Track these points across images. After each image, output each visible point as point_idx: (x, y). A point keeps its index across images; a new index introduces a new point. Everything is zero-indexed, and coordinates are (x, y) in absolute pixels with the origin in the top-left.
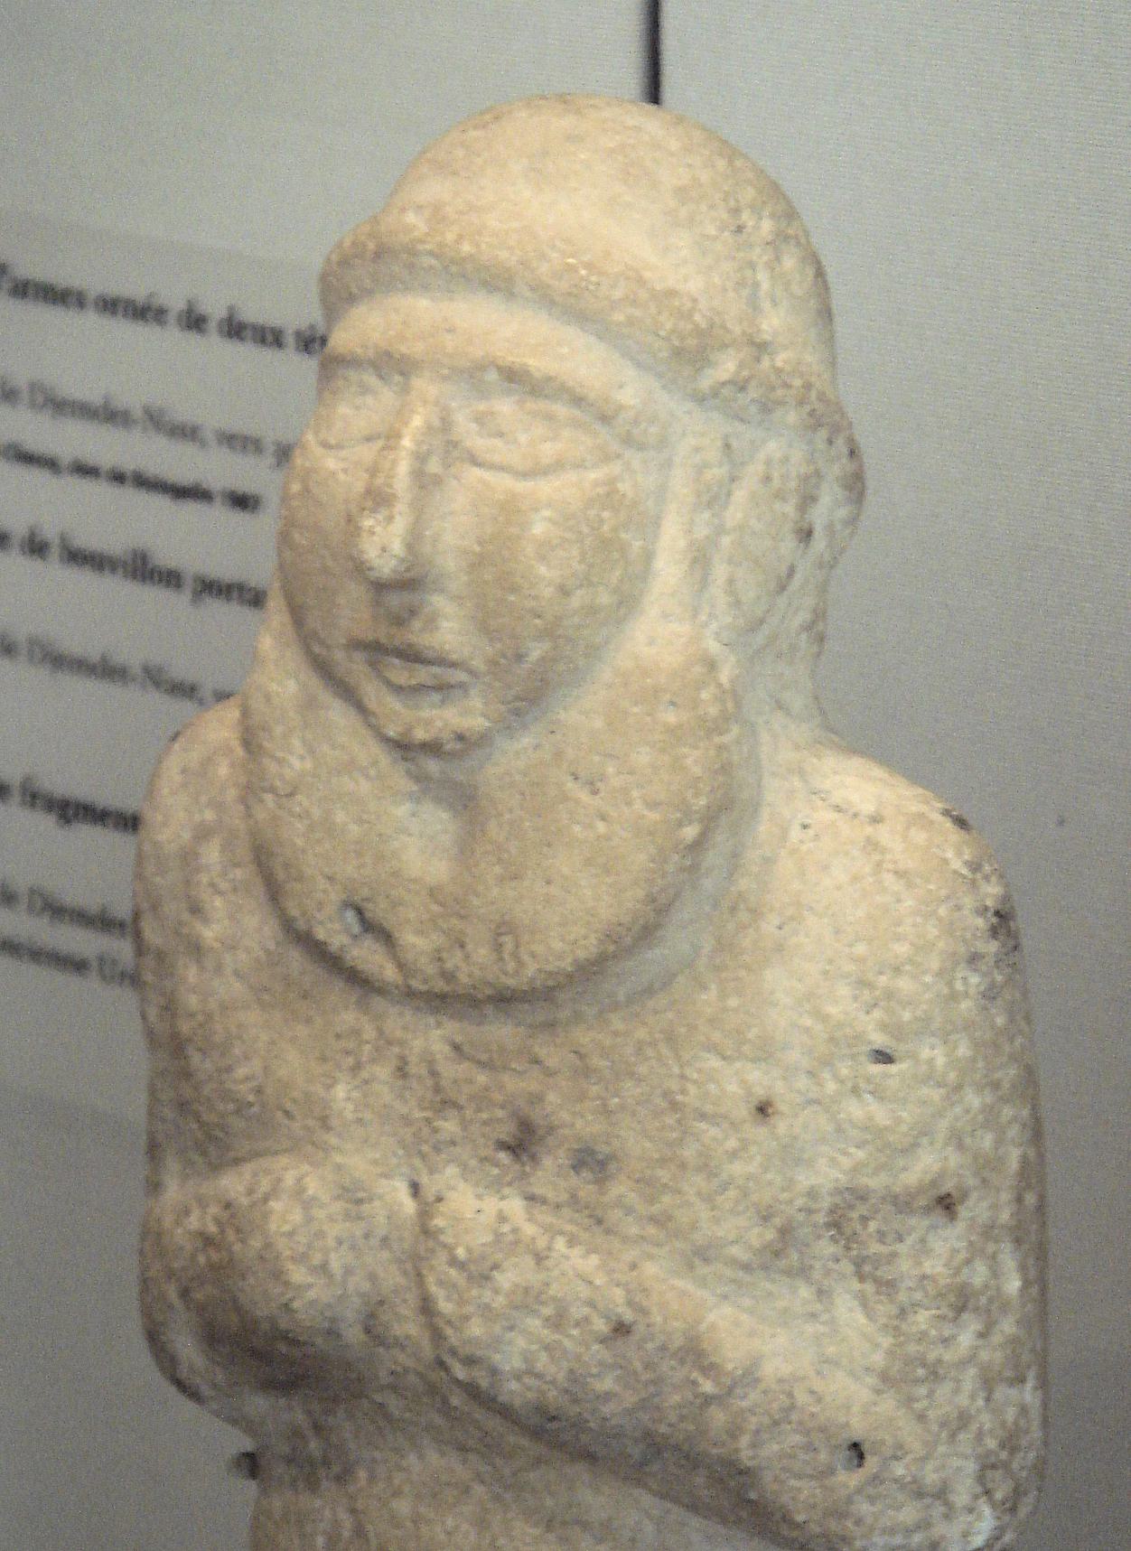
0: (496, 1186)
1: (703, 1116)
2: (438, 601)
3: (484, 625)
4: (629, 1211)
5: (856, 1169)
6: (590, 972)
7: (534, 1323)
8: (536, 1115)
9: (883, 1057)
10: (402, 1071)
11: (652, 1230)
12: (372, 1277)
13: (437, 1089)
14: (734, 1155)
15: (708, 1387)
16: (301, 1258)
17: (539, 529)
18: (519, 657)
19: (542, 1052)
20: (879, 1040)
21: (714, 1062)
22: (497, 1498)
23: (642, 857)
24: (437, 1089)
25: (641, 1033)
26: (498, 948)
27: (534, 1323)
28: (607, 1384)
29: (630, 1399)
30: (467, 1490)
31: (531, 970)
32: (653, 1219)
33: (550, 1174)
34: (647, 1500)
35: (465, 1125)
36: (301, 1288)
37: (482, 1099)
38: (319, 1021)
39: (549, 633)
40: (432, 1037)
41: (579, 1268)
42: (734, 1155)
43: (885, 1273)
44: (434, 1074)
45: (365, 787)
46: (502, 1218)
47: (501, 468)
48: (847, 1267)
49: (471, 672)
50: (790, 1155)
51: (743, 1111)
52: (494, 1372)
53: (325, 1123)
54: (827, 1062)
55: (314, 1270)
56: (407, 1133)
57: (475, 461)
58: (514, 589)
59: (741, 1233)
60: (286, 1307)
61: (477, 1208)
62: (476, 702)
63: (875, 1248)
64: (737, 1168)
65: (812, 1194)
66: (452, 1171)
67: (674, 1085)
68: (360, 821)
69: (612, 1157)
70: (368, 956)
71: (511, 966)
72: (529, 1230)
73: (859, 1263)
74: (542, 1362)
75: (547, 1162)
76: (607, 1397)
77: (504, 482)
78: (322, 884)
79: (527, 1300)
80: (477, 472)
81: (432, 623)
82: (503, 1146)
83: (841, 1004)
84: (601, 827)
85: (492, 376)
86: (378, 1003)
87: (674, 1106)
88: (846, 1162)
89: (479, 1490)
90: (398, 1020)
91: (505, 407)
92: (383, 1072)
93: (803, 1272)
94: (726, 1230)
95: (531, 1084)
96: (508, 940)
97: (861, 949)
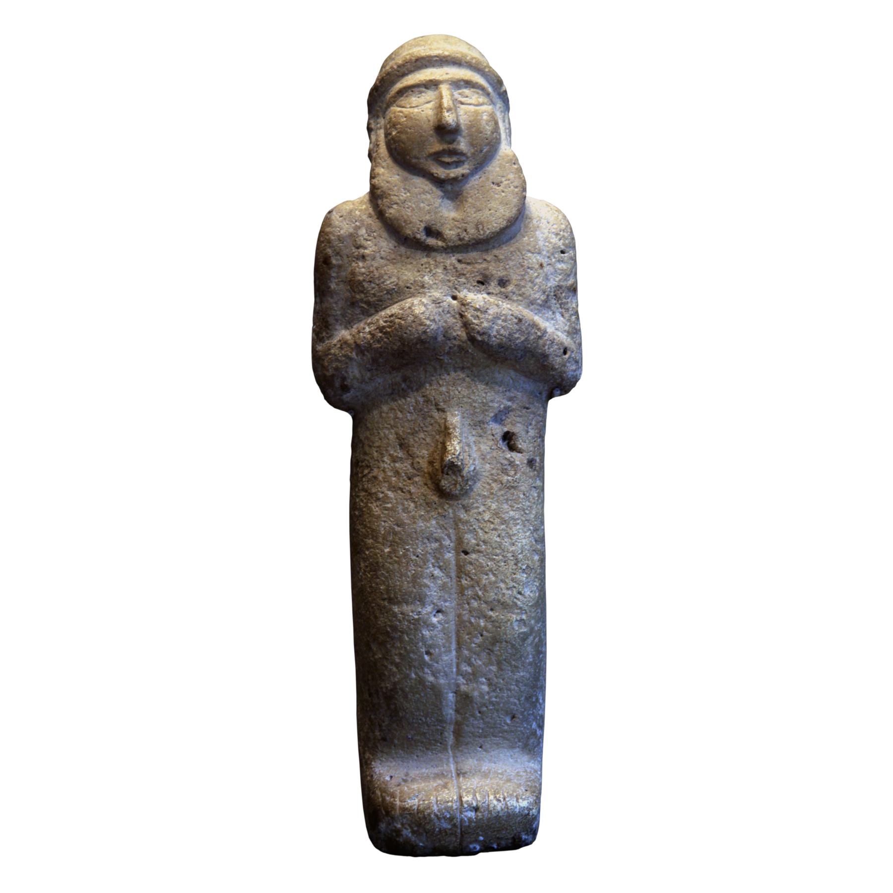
0: (480, 292)
1: (529, 268)
2: (460, 138)
3: (472, 144)
4: (514, 293)
5: (560, 281)
6: (503, 231)
7: (500, 322)
8: (487, 273)
9: (563, 252)
10: (445, 268)
11: (520, 298)
12: (446, 322)
13: (457, 271)
14: (537, 277)
15: (539, 334)
16: (428, 319)
17: (485, 117)
18: (481, 151)
19: (485, 257)
20: (563, 247)
21: (529, 254)
22: (473, 380)
23: (515, 200)
24: (457, 271)
25: (511, 249)
26: (477, 229)
27: (500, 322)
28: (517, 335)
29: (523, 338)
30: (464, 380)
31: (488, 232)
32: (520, 295)
33: (493, 287)
34: (512, 373)
35: (466, 278)
36: (429, 326)
37: (472, 272)
38: (414, 263)
39: (488, 144)
40: (452, 260)
41: (506, 307)
42: (537, 277)
43: (566, 307)
44: (455, 268)
45: (429, 196)
46: (484, 298)
47: (470, 104)
48: (558, 306)
49: (467, 158)
50: (547, 278)
51: (537, 266)
52: (489, 335)
53: (423, 287)
54: (553, 254)
55: (431, 321)
56: (450, 284)
57: (462, 103)
58: (481, 133)
59: (540, 297)
60: (425, 332)
61: (476, 298)
62: (466, 166)
63: (564, 300)
64: (538, 280)
65: (550, 287)
66: (465, 291)
67: (521, 261)
68: (429, 205)
69: (509, 281)
70: (431, 241)
71: (482, 232)
72: (492, 300)
73: (561, 304)
74: (502, 332)
75: (492, 284)
76: (518, 338)
77: (472, 108)
78: (418, 223)
79: (497, 317)
80: (462, 106)
81: (459, 143)
82: (479, 282)
83: (555, 240)
84: (503, 194)
85: (462, 83)
86: (433, 254)
87: (522, 266)
88: (557, 279)
89: (467, 379)
90: (440, 258)
91: (467, 91)
92: (439, 270)
93: (549, 308)
94: (537, 296)
95: (484, 265)
96: (480, 227)
97: (555, 226)
